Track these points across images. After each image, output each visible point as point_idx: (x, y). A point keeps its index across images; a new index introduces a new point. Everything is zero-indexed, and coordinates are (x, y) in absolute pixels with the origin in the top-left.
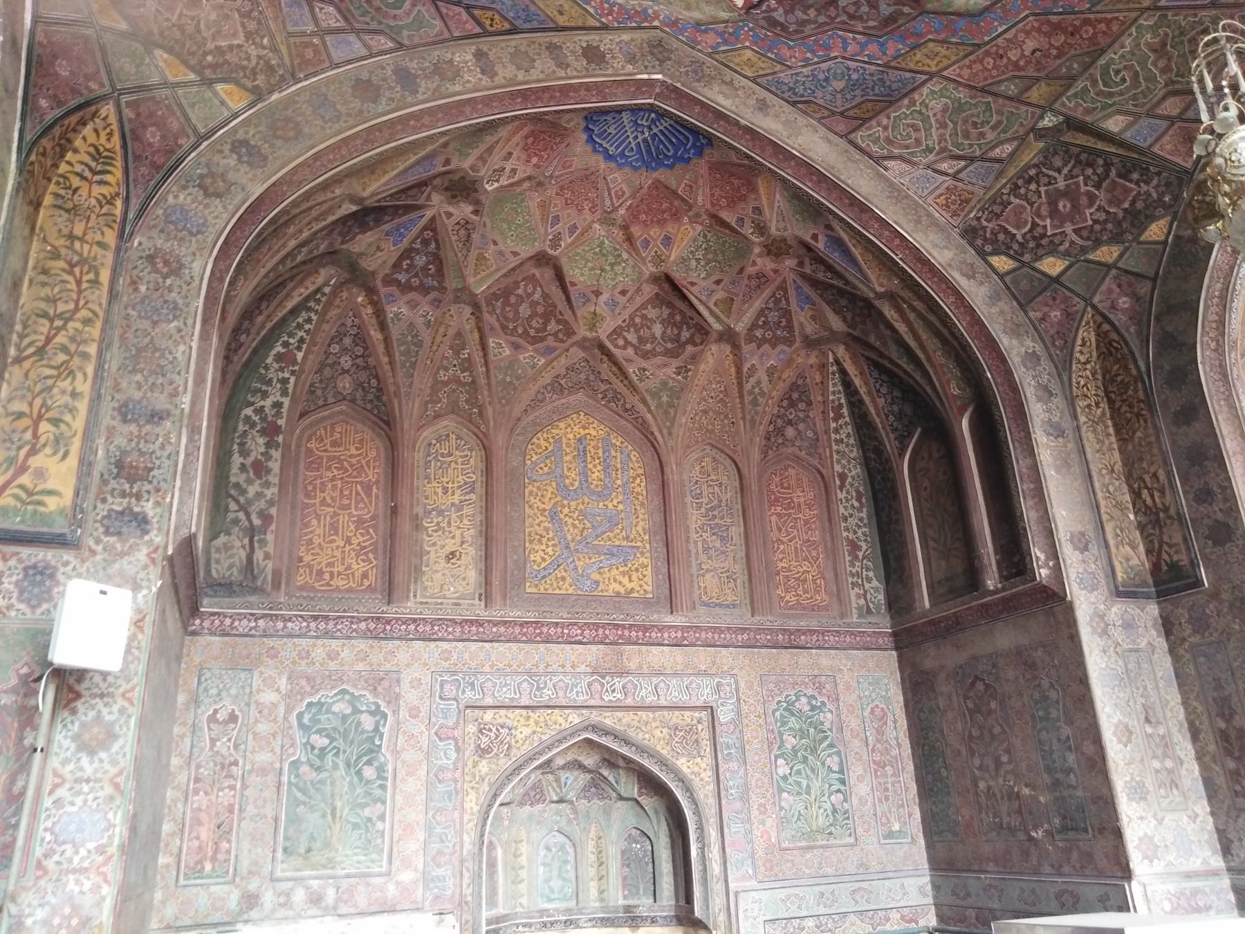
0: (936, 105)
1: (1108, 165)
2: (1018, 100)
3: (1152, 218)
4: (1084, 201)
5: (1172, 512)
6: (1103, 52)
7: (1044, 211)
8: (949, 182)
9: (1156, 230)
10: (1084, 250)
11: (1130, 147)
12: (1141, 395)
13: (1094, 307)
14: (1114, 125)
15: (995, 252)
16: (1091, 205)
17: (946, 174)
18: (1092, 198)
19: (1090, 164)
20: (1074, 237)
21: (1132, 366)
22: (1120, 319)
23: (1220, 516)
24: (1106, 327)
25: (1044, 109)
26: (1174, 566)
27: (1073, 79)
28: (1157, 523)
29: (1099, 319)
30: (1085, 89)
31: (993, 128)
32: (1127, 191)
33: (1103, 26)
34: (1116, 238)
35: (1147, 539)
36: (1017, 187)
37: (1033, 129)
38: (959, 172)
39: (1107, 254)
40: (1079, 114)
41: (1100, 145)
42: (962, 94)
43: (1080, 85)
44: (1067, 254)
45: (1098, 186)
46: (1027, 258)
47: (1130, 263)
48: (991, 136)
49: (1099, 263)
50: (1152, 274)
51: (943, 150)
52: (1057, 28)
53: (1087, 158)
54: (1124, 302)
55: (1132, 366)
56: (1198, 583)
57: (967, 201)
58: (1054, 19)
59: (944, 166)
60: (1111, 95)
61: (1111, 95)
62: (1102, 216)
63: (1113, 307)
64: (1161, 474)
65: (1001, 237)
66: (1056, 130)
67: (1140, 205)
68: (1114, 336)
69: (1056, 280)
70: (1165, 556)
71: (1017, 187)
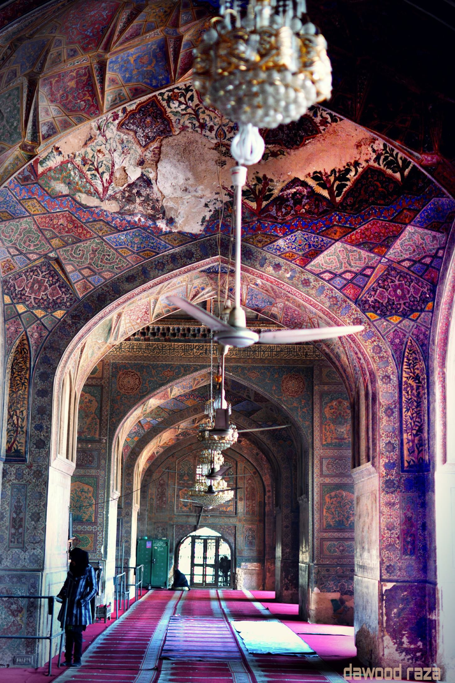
0: (24, 226)
1: (58, 280)
2: (48, 240)
3: (59, 308)
4: (43, 288)
5: (24, 429)
6: (80, 241)
7: (29, 285)
8: (10, 258)
9: (59, 314)
10: (33, 307)
11: (69, 280)
12: (27, 376)
13: (26, 333)
14: (69, 268)
15: (7, 294)
16: (44, 291)
17: (10, 254)
18: (46, 289)
19: (53, 276)
20: (32, 300)
21: (28, 363)
22: (32, 341)
23: (42, 437)
24: (25, 342)
25: (54, 250)
26: (17, 451)
27: (66, 244)
28: (17, 431)
29: (25, 337)
30: (68, 250)
31: (35, 245)
32: (58, 293)
33: (85, 232)
34: (45, 309)
35: (9, 436)
36: (27, 272)
37: (46, 255)
38: (14, 255)
39: (39, 313)
40: (61, 258)
41: (60, 272)
42: (34, 227)
43: (68, 248)
44: (28, 306)
45: (50, 286)
46: (15, 301)
47: (45, 321)
48: (32, 248)
49: (35, 316)
50: (50, 330)
51: (15, 244)
52: (72, 221)
53: (52, 274)
54: (36, 335)
55: (28, 363)
56: (24, 461)
57: (11, 269)
58: (74, 218)
59: (11, 250)
60: (74, 257)
61: (74, 257)
62: (45, 297)
63: (32, 335)
64: (25, 413)
65: (12, 288)
66: (50, 258)
67: (59, 301)
68: (27, 347)
69: (19, 315)
70: (15, 446)
71: (27, 272)
